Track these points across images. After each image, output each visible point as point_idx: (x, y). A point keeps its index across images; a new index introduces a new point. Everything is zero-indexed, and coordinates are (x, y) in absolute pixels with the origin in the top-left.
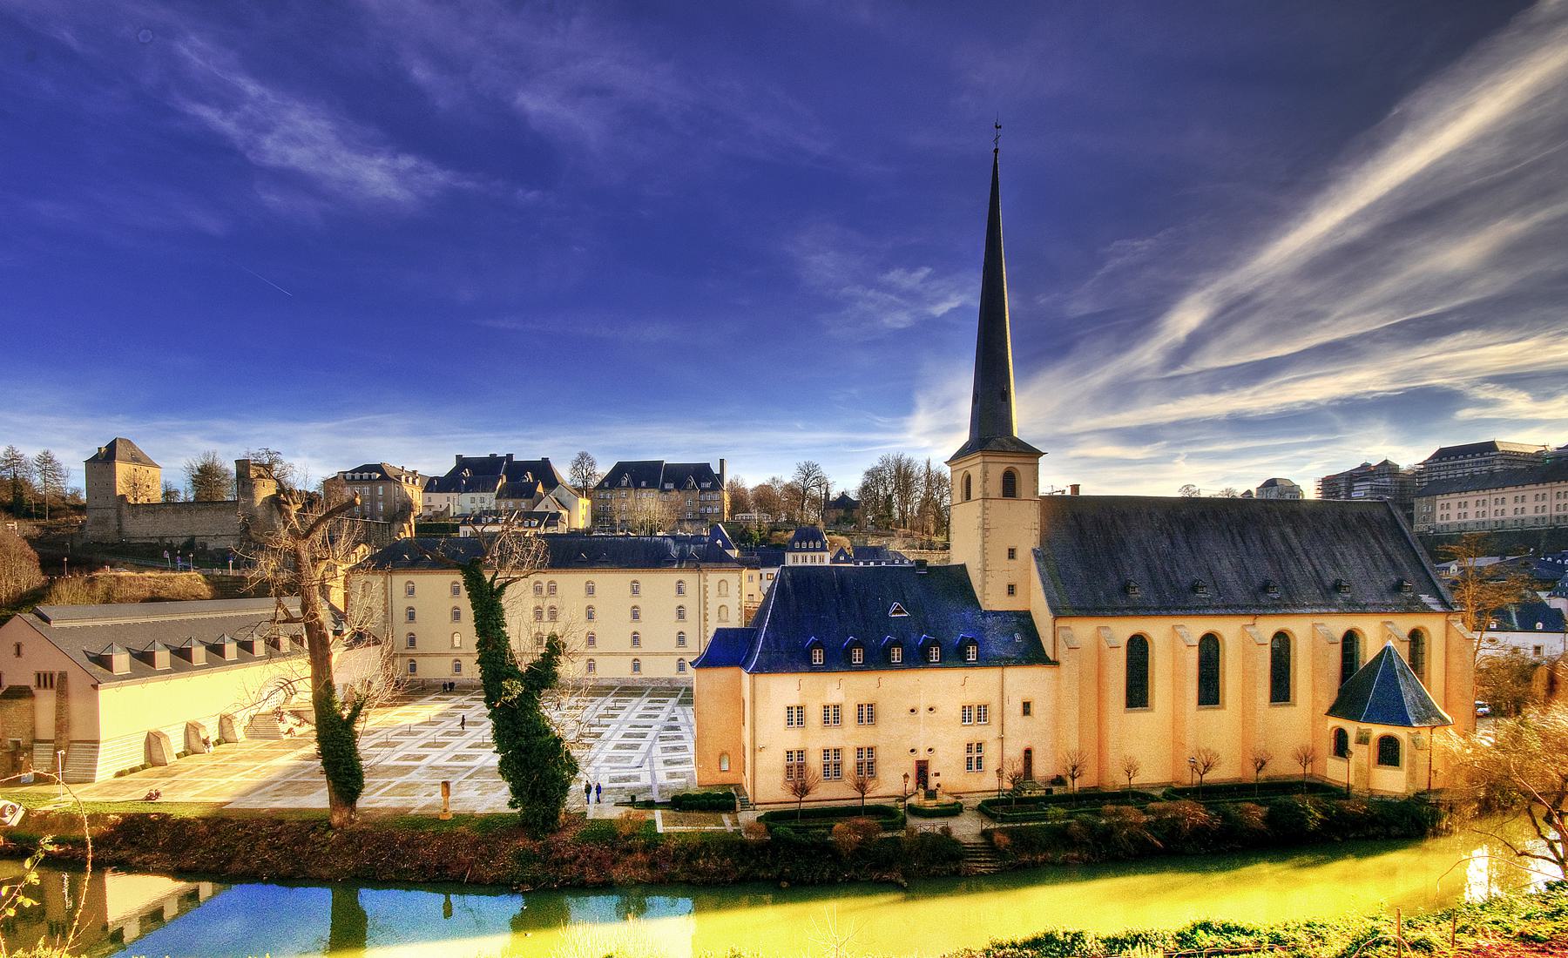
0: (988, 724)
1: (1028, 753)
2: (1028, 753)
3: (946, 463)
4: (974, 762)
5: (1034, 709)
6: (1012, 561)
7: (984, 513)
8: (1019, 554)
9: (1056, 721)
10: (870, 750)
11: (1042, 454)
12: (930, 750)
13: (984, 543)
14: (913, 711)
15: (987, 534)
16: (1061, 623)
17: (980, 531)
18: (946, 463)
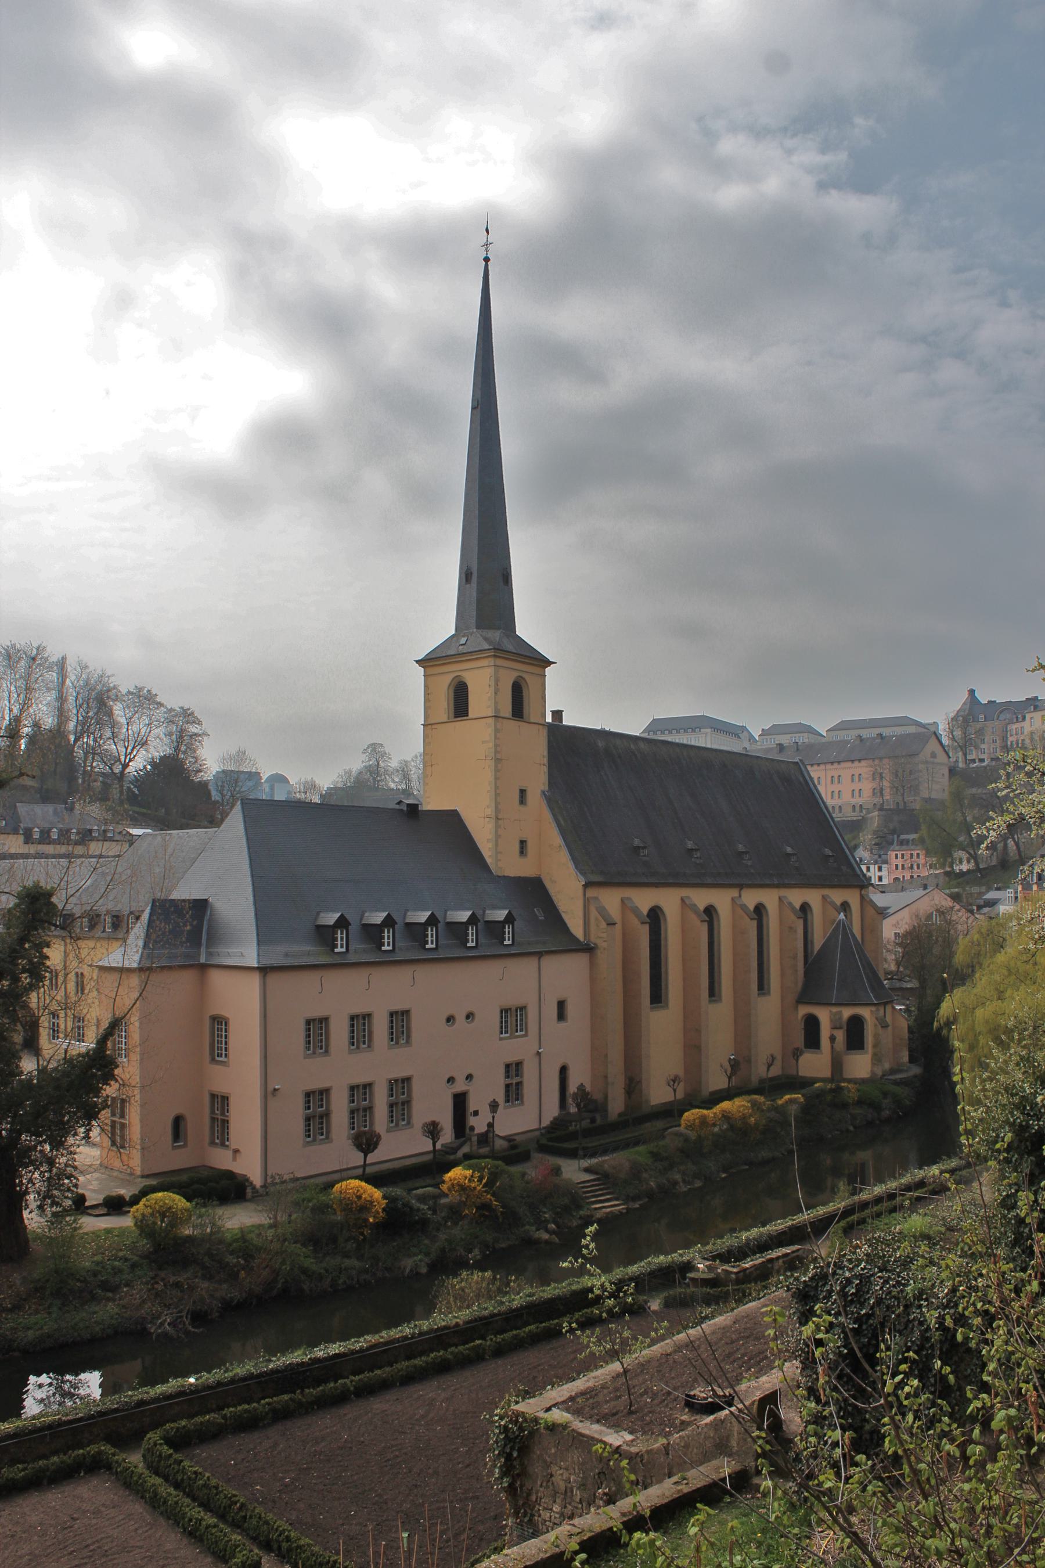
0: (526, 1035)
1: (563, 1070)
2: (563, 1070)
3: (417, 662)
4: (513, 1093)
5: (570, 1010)
6: (522, 808)
7: (496, 738)
8: (530, 797)
9: (596, 1018)
10: (407, 1080)
11: (549, 663)
12: (469, 1077)
13: (496, 779)
14: (448, 1020)
15: (499, 765)
16: (592, 892)
17: (492, 763)
18: (417, 662)
